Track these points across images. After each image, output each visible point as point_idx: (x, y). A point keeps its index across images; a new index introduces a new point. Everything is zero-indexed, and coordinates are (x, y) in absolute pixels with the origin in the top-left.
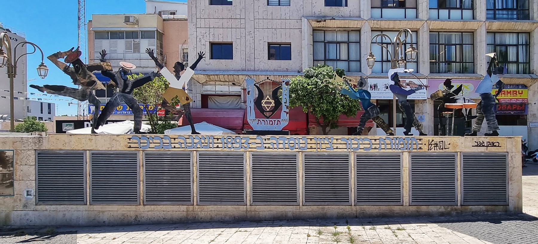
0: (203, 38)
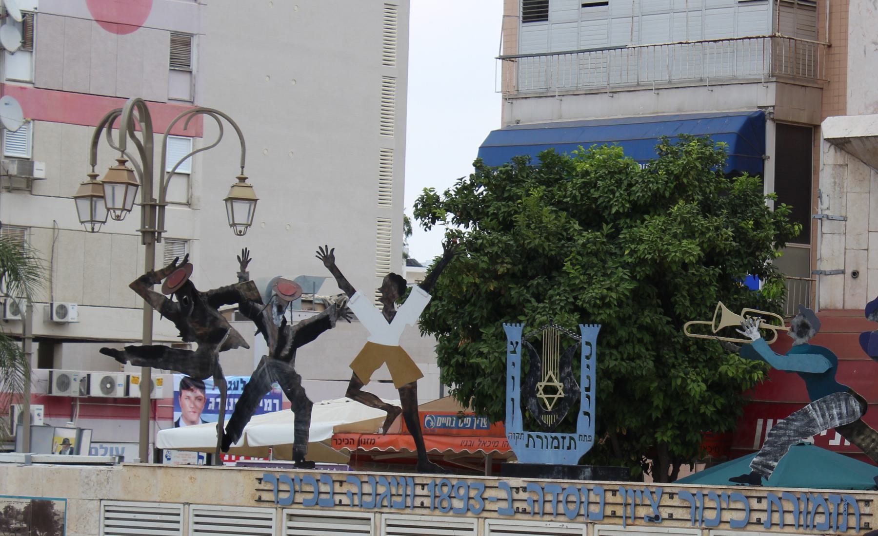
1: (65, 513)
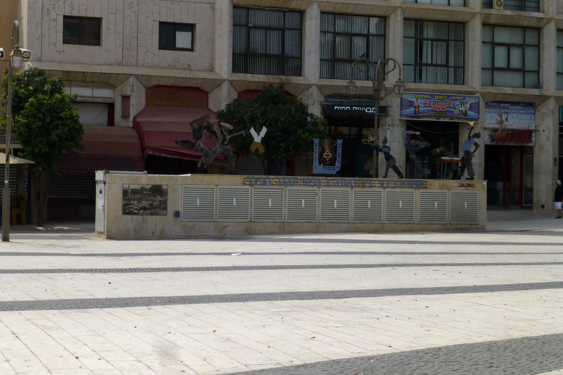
0: (54, 8)
1: (167, 189)
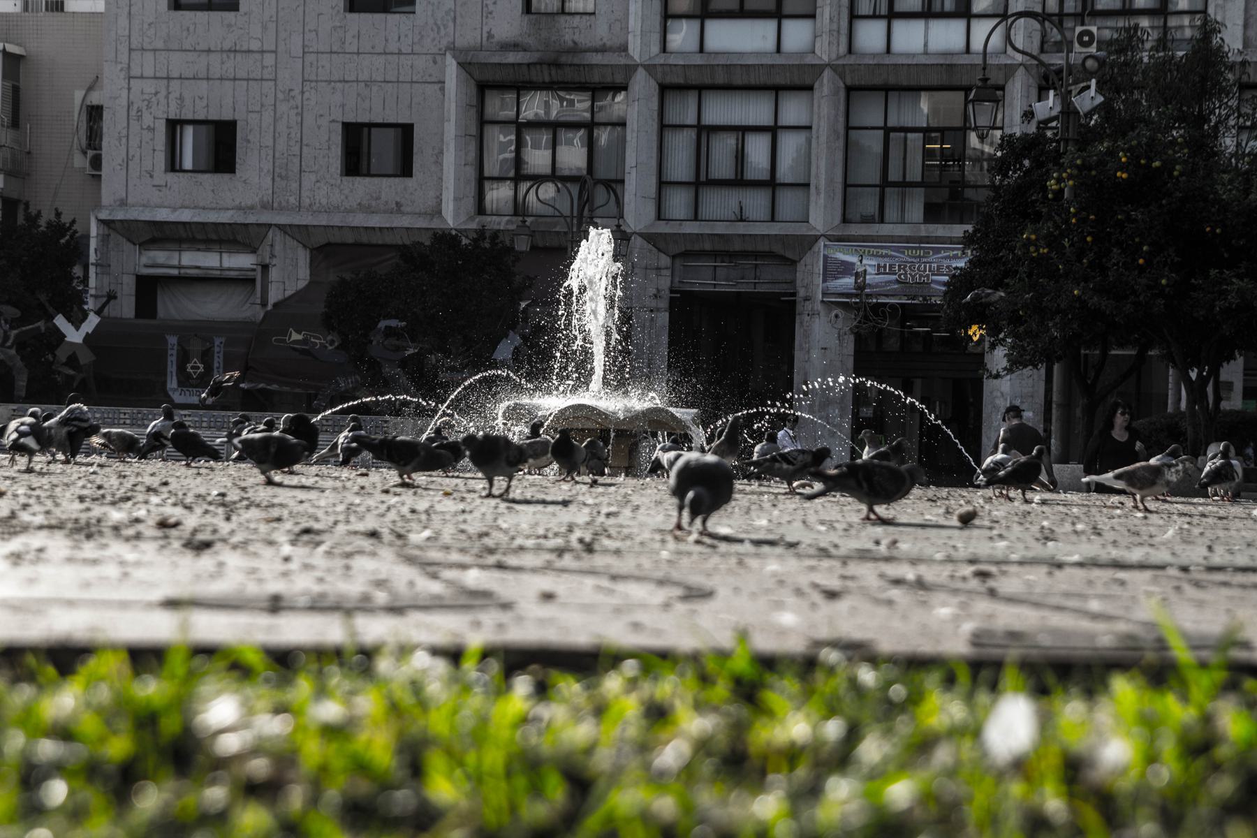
0: (148, 107)
